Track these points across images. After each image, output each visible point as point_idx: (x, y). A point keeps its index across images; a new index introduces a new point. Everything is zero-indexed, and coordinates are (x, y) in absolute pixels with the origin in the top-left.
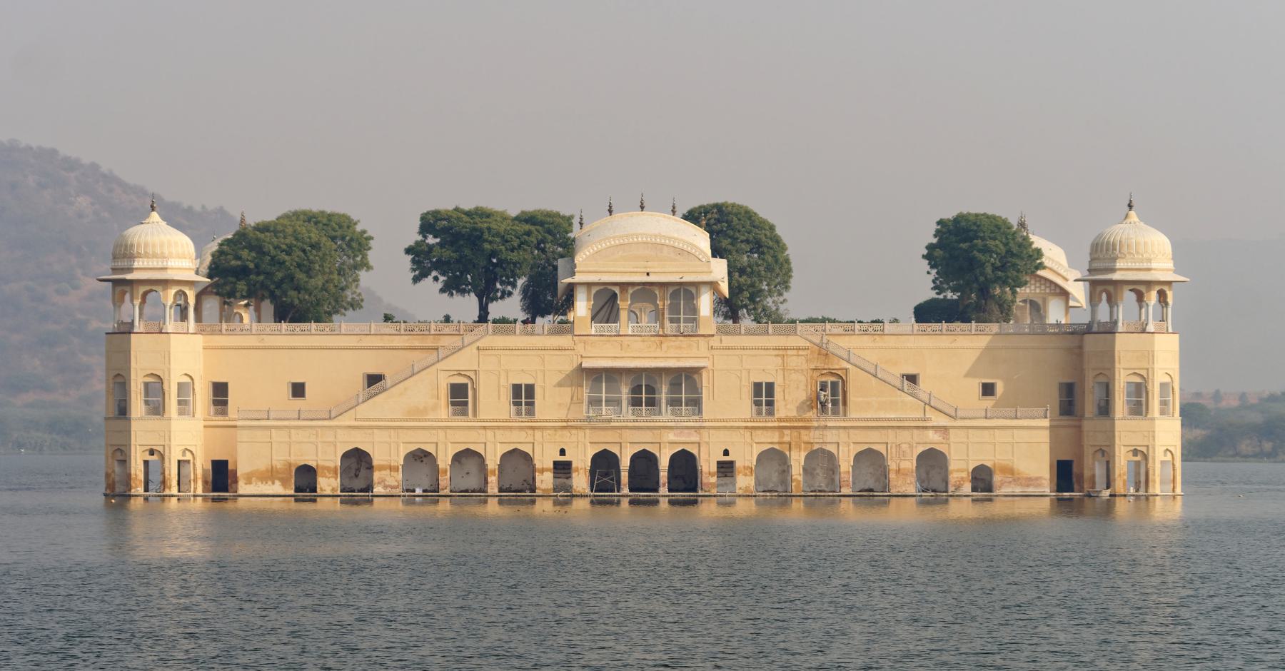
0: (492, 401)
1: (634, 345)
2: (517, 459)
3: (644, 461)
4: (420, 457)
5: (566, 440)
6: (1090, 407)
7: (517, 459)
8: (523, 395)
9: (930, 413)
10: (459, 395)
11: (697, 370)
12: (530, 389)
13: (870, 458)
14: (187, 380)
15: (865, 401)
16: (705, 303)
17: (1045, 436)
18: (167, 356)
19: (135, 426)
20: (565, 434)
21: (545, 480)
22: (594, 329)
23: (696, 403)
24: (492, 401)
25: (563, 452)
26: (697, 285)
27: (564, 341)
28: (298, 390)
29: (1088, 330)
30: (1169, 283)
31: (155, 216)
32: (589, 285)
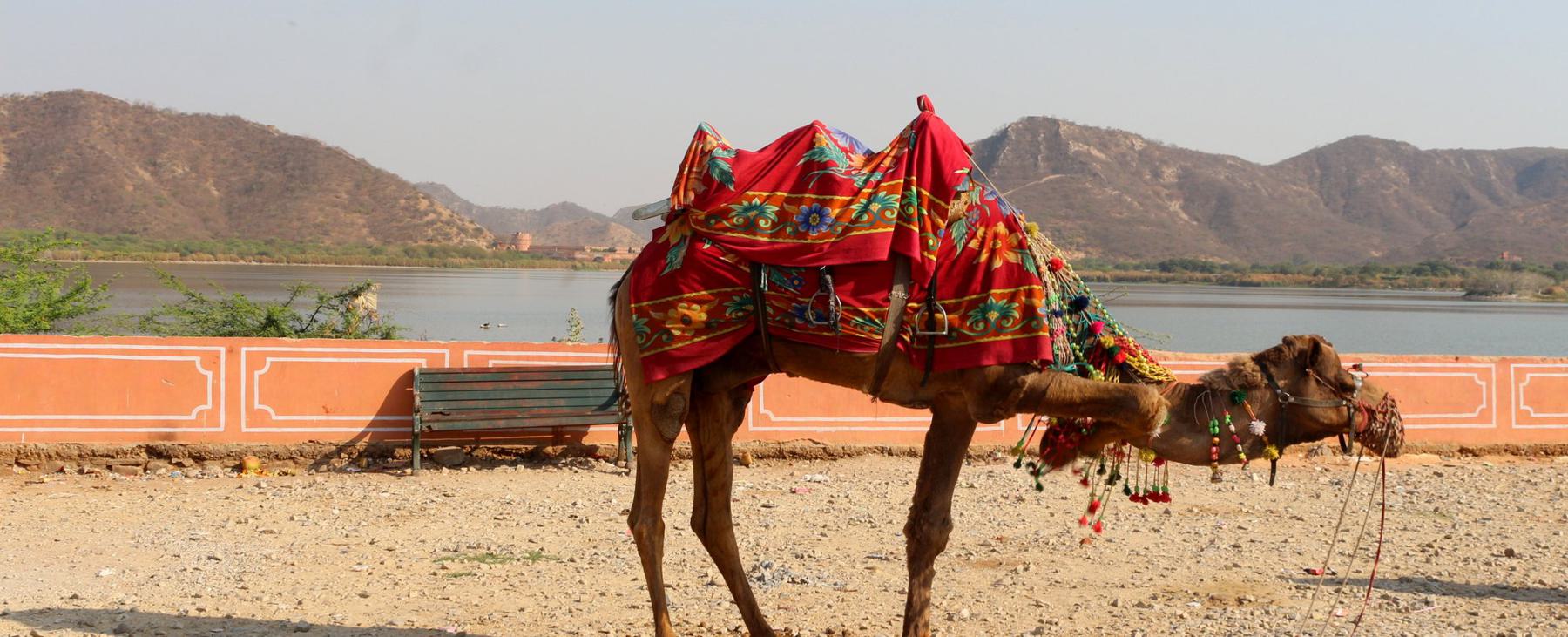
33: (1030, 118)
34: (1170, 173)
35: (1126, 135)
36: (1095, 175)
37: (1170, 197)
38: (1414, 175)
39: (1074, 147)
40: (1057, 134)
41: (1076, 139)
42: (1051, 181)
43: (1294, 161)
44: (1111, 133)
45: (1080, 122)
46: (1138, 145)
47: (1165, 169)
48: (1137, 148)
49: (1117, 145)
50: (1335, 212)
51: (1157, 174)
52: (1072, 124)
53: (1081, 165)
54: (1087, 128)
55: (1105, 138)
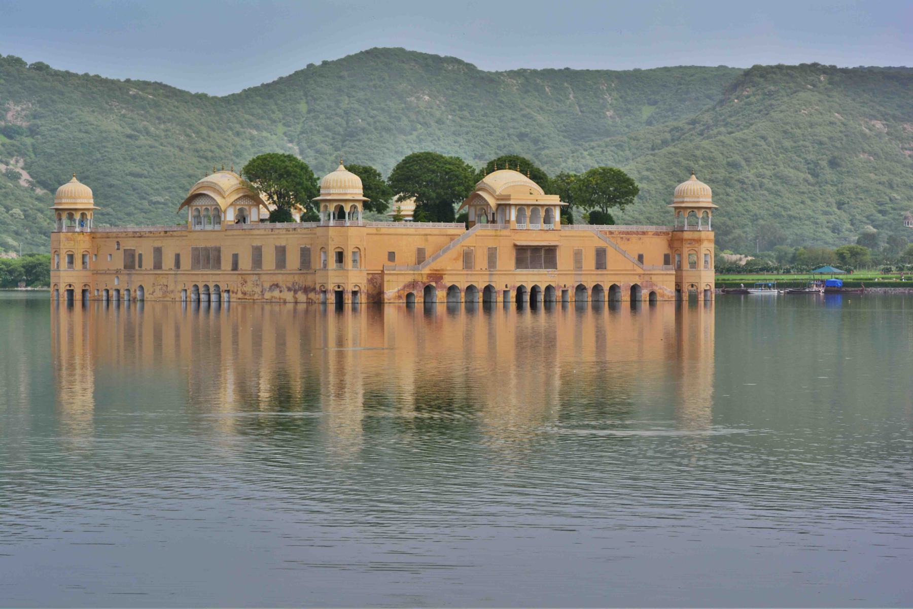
0: (481, 261)
1: (535, 235)
2: (488, 290)
3: (534, 290)
4: (452, 290)
6: (686, 266)
7: (488, 290)
9: (636, 267)
10: (468, 258)
13: (613, 289)
14: (356, 250)
17: (673, 278)
19: (330, 273)
20: (510, 277)
22: (517, 226)
24: (481, 261)
25: (506, 286)
26: (555, 206)
27: (505, 232)
28: (391, 256)
30: (710, 208)
31: (342, 167)
32: (516, 205)
47: (11, 104)
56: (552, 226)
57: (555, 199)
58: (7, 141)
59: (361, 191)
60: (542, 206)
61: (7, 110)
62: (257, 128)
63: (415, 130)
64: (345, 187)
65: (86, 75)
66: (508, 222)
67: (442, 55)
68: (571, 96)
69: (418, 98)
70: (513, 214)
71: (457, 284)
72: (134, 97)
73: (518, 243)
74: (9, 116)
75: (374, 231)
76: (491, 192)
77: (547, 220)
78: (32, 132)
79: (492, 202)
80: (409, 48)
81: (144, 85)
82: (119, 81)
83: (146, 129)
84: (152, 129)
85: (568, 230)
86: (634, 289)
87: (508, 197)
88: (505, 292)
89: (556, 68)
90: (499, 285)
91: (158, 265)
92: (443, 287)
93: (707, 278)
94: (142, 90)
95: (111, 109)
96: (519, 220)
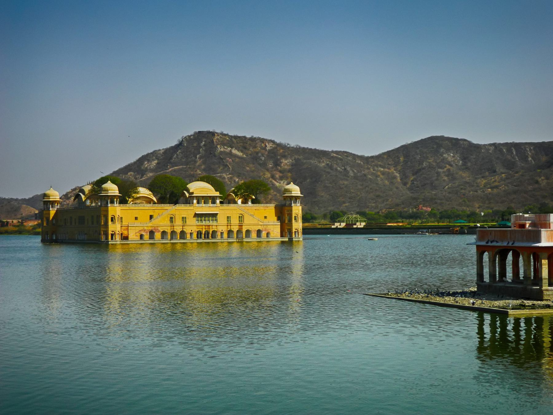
5: (191, 228)
8: (184, 219)
11: (217, 214)
12: (185, 218)
15: (247, 220)
16: (218, 201)
18: (116, 211)
21: (188, 236)
22: (197, 205)
23: (216, 220)
28: (136, 218)
29: (285, 205)
31: (109, 182)
33: (199, 132)
34: (286, 163)
35: (263, 140)
36: (226, 166)
37: (281, 178)
38: (464, 159)
39: (220, 149)
40: (213, 141)
41: (223, 144)
42: (175, 171)
43: (389, 154)
44: (252, 139)
45: (231, 134)
46: (269, 146)
48: (268, 148)
49: (255, 147)
50: (405, 184)
51: (277, 164)
52: (227, 135)
53: (221, 160)
54: (236, 137)
55: (243, 143)
56: (215, 205)
57: (217, 194)
58: (281, 175)
59: (118, 192)
60: (210, 197)
61: (281, 163)
62: (384, 167)
63: (446, 167)
64: (107, 191)
65: (315, 149)
66: (193, 203)
67: (459, 138)
68: (514, 153)
69: (448, 155)
70: (195, 201)
71: (166, 230)
72: (333, 157)
73: (197, 213)
74: (282, 165)
75: (128, 208)
76: (188, 190)
77: (214, 202)
78: (289, 171)
79: (187, 195)
80: (446, 136)
81: (337, 152)
82: (328, 151)
83: (336, 169)
84: (339, 169)
85: (225, 206)
86: (259, 232)
87: (193, 193)
88: (191, 234)
89: (509, 142)
90: (188, 230)
91: (71, 223)
92: (159, 231)
93: (298, 225)
94: (337, 154)
95: (323, 162)
96: (198, 203)
